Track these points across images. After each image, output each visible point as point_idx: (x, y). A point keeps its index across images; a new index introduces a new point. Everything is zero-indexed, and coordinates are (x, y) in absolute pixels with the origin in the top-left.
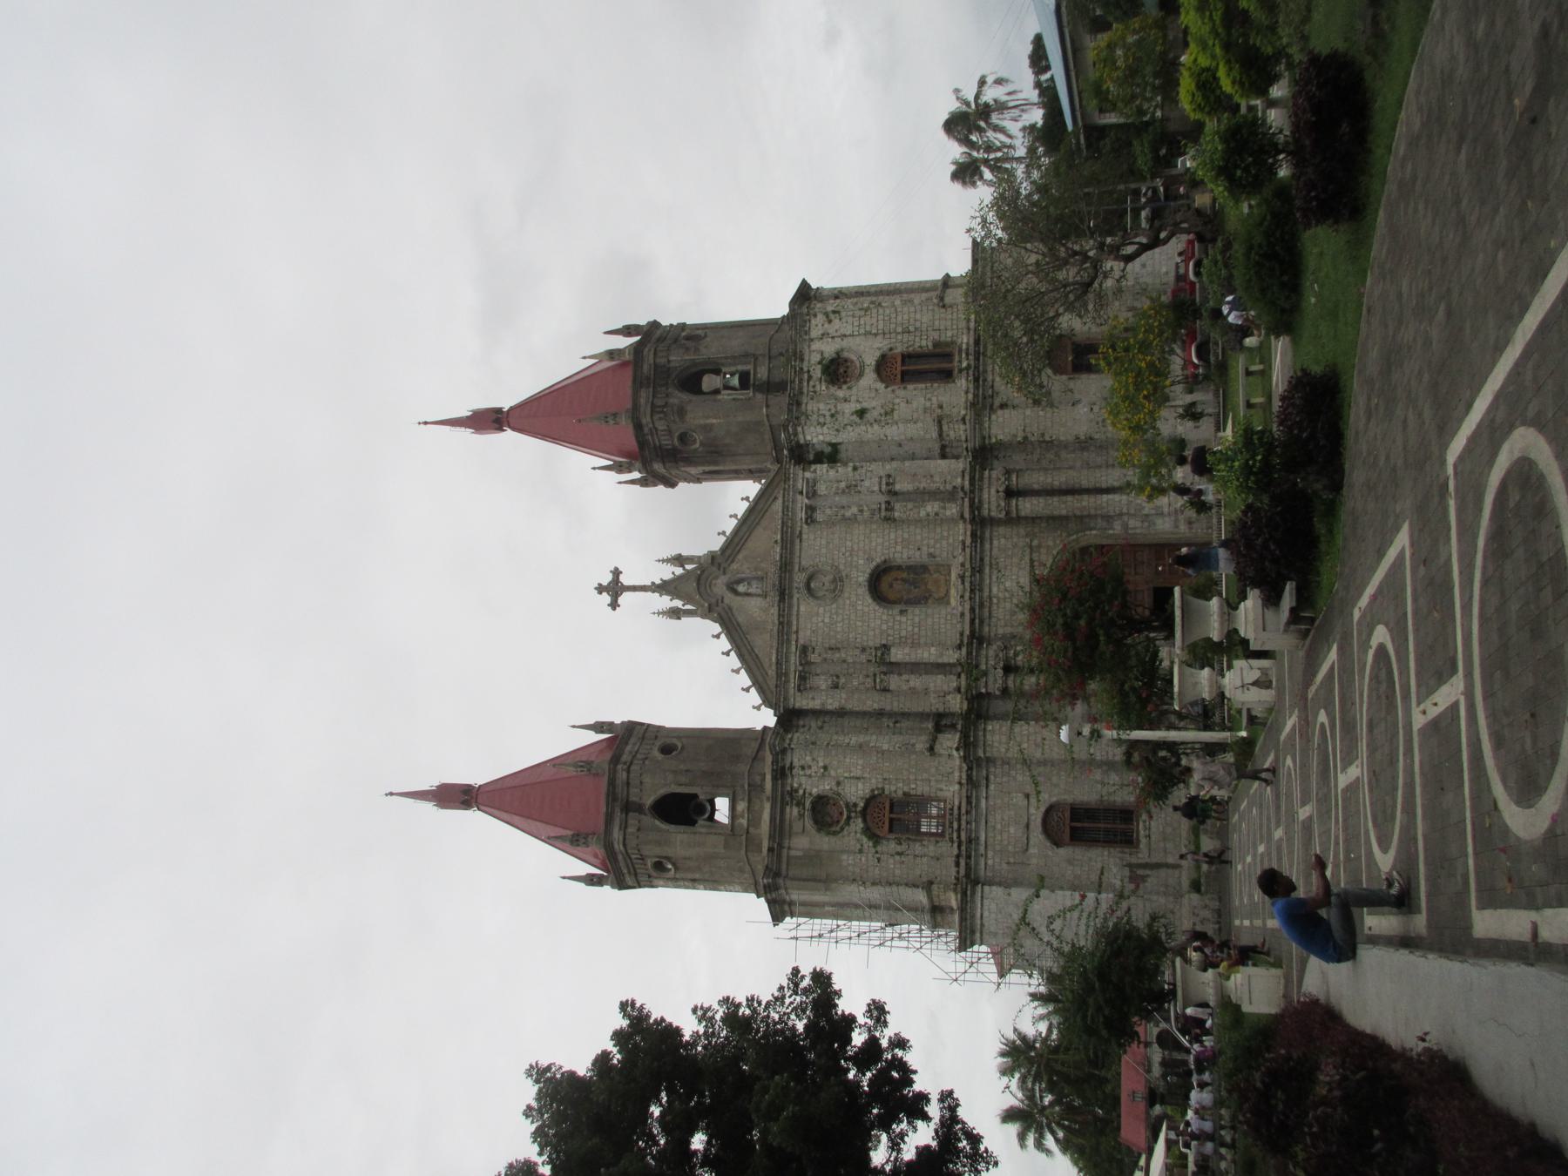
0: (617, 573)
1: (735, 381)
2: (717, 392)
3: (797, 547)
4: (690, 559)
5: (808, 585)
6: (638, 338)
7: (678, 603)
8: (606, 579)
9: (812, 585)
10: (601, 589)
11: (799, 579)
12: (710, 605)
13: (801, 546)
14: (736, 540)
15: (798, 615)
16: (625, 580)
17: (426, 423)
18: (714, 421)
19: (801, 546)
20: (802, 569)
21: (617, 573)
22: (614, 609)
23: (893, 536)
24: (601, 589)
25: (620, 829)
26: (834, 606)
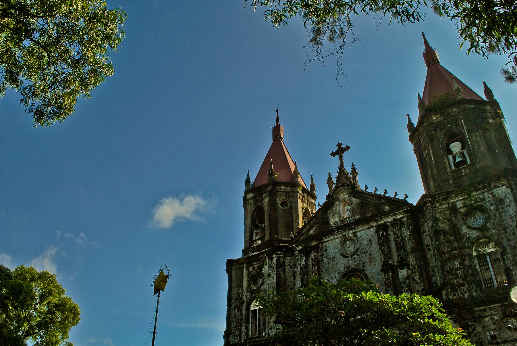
0: (348, 148)
1: (458, 160)
2: (450, 152)
3: (366, 227)
4: (355, 178)
5: (349, 239)
6: (485, 99)
7: (334, 180)
8: (344, 146)
9: (348, 242)
10: (339, 145)
11: (349, 234)
12: (332, 196)
13: (366, 229)
14: (364, 196)
15: (334, 239)
16: (345, 155)
17: (423, 35)
18: (432, 159)
19: (366, 229)
20: (355, 234)
21: (348, 148)
22: (331, 155)
23: (378, 277)
24: (339, 145)
25: (251, 197)
26: (339, 256)
